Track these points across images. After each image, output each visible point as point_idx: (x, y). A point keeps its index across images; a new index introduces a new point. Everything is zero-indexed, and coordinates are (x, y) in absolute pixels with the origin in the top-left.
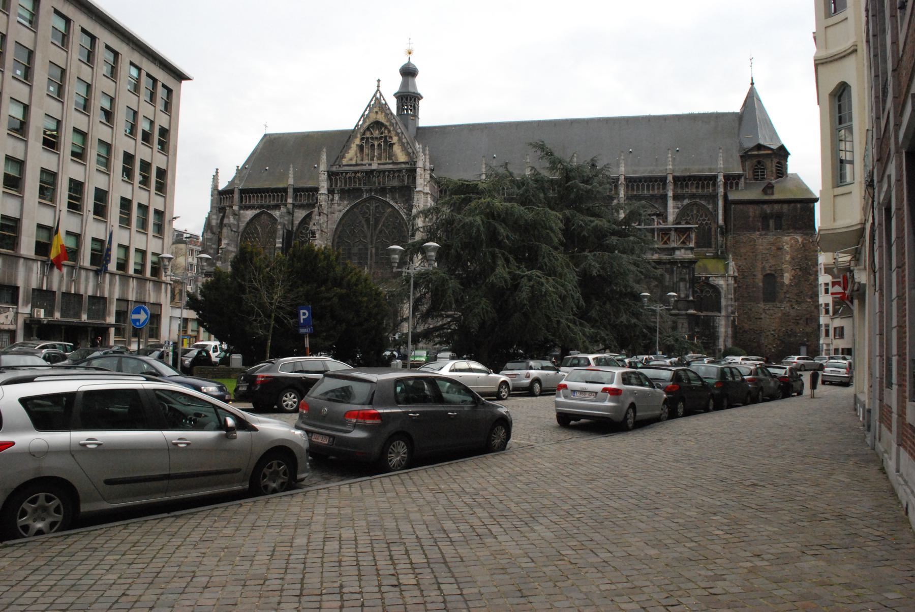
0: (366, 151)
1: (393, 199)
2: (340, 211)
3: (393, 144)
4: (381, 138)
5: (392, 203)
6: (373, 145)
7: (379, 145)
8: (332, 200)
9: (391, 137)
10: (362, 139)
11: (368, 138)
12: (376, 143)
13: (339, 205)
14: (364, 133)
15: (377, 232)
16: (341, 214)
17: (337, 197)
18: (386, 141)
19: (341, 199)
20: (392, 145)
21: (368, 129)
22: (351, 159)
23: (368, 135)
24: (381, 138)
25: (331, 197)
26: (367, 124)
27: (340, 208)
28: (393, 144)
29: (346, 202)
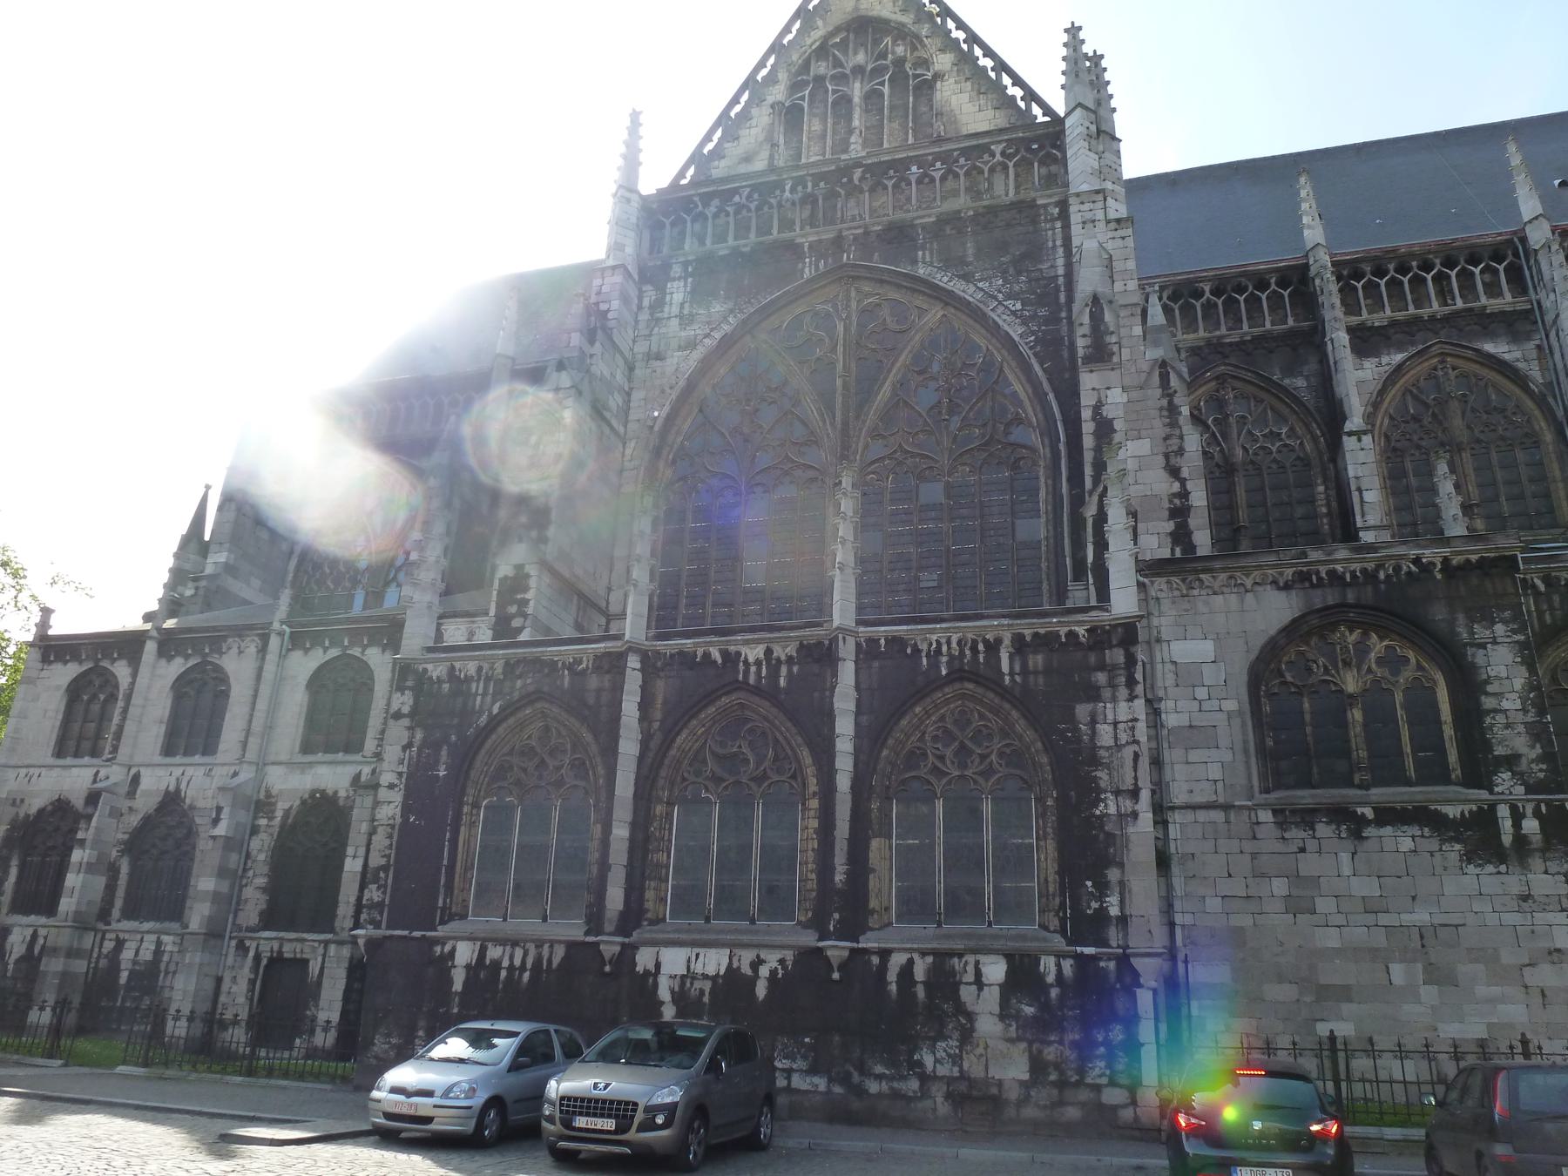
0: (812, 125)
1: (949, 262)
2: (691, 345)
3: (938, 76)
4: (878, 71)
5: (943, 280)
6: (844, 101)
7: (872, 97)
8: (659, 304)
9: (925, 63)
10: (795, 87)
11: (820, 80)
12: (857, 90)
13: (685, 320)
14: (806, 66)
15: (871, 417)
16: (697, 354)
17: (677, 293)
18: (899, 79)
19: (697, 295)
20: (926, 87)
21: (822, 51)
22: (747, 159)
23: (821, 68)
24: (878, 71)
25: (650, 294)
26: (817, 34)
27: (689, 332)
28: (938, 76)
29: (717, 308)
